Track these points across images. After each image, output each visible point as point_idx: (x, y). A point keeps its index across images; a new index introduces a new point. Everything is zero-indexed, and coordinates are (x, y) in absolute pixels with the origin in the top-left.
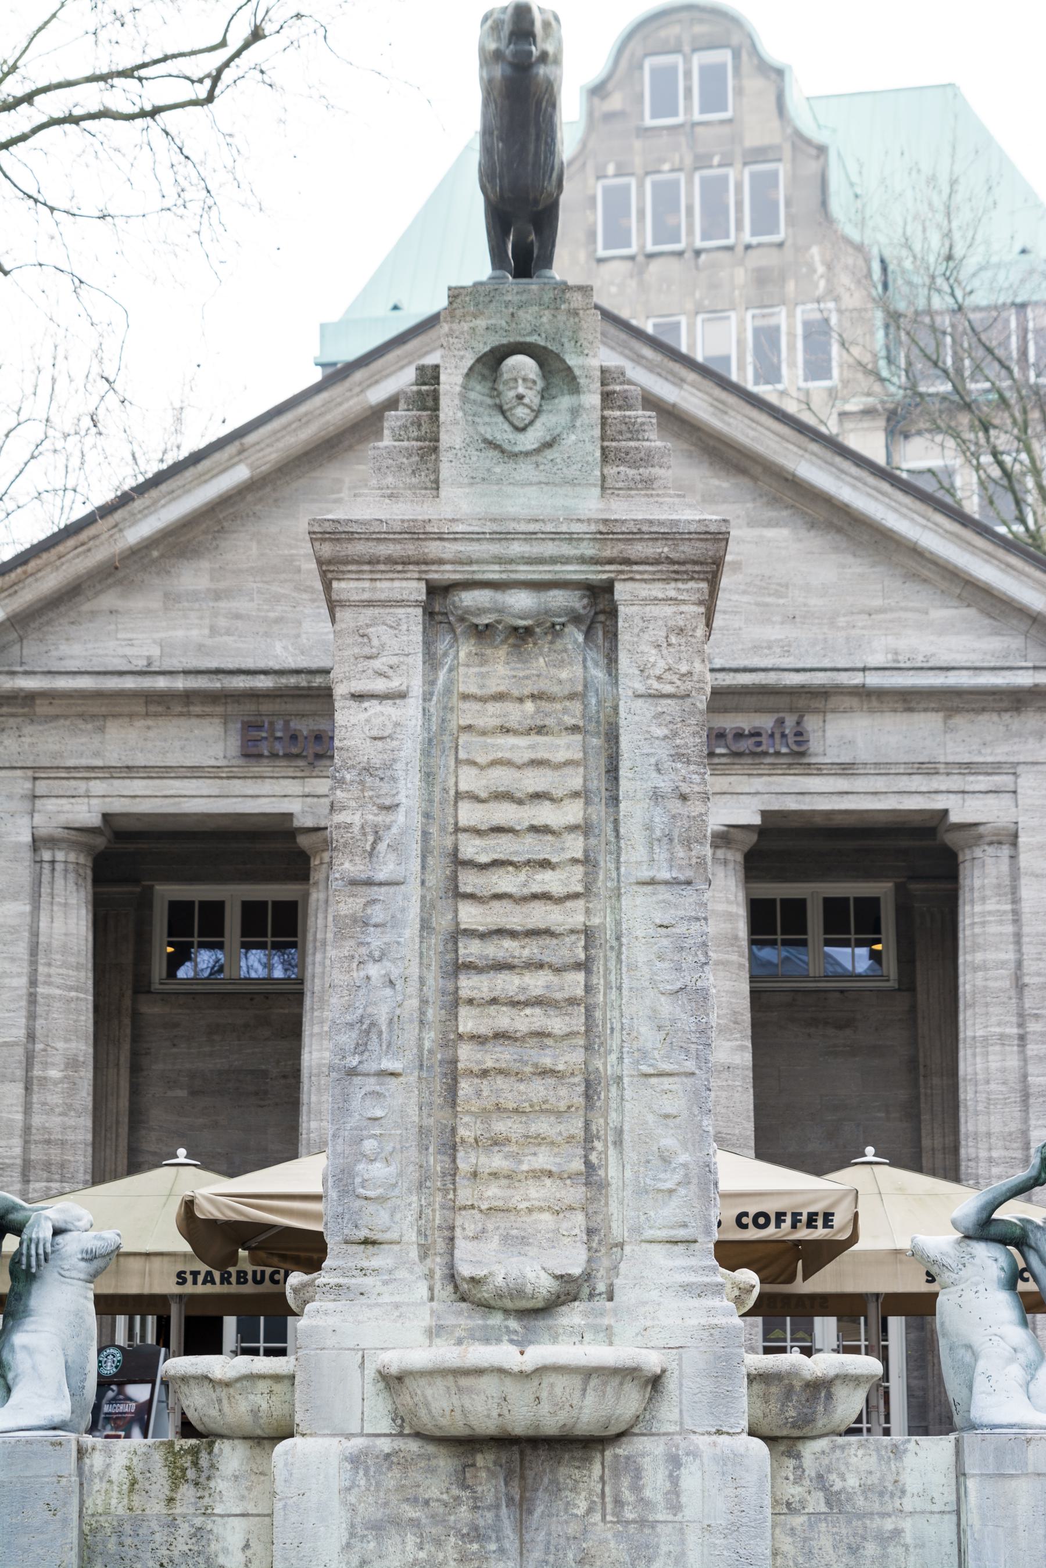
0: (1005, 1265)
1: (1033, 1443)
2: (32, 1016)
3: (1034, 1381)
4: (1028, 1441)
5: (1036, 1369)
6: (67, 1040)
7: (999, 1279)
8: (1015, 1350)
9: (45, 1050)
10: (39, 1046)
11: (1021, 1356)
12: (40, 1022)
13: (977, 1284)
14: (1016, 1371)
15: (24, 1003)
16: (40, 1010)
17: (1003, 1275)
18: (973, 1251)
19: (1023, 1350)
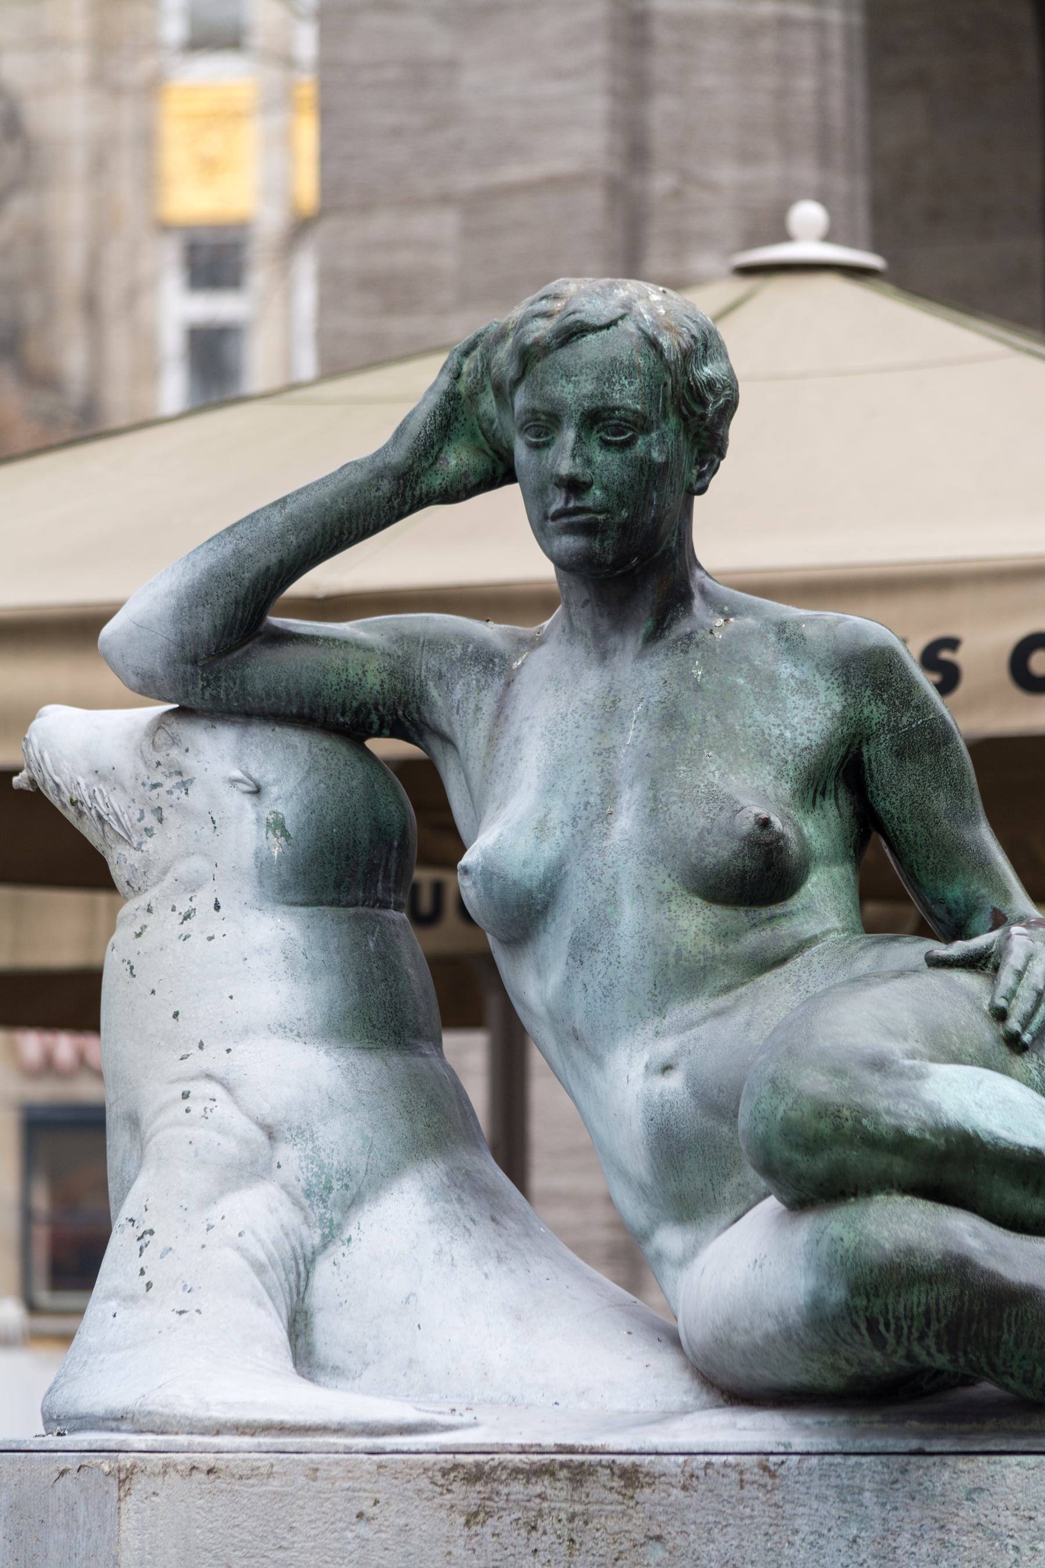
0: (289, 811)
1: (140, 1484)
2: (633, 88)
3: (336, 1250)
4: (125, 1478)
5: (353, 1202)
6: (746, 157)
7: (262, 864)
8: (271, 1134)
9: (677, 194)
10: (661, 182)
11: (289, 1155)
12: (662, 109)
13: (192, 886)
14: (260, 1213)
15: (599, 49)
16: (662, 65)
17: (276, 847)
18: (189, 762)
19: (302, 1133)
